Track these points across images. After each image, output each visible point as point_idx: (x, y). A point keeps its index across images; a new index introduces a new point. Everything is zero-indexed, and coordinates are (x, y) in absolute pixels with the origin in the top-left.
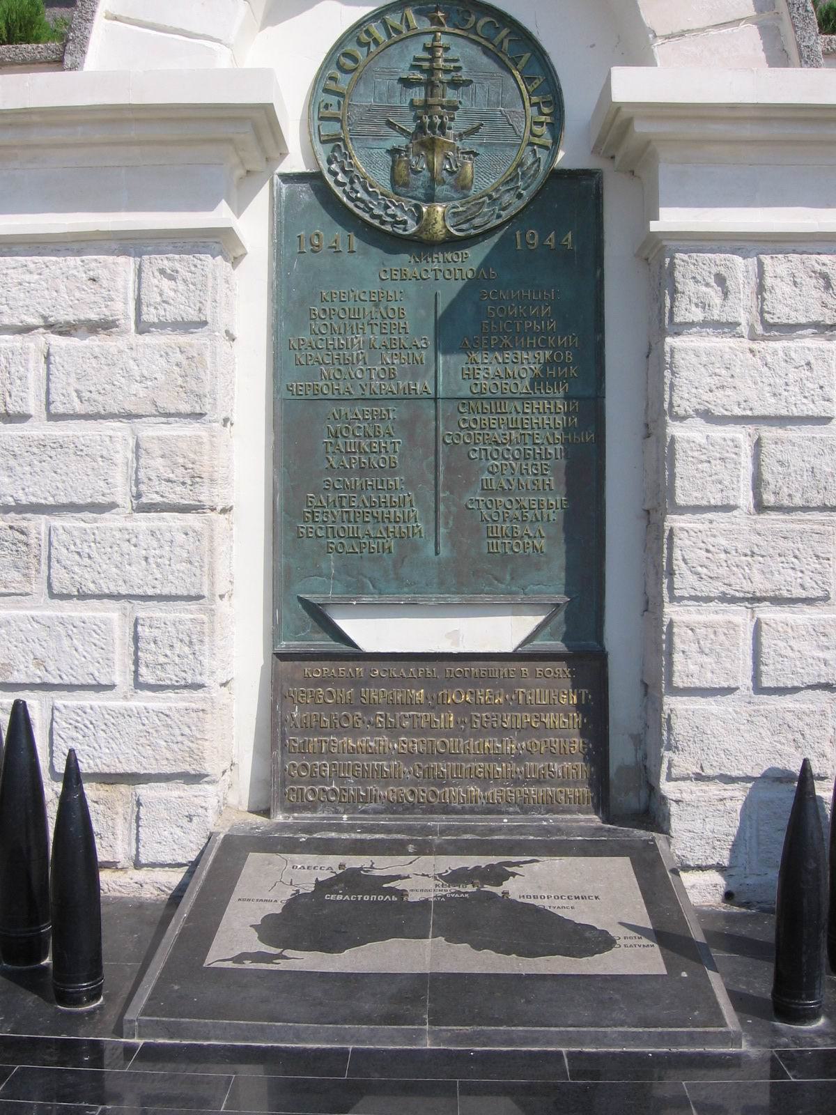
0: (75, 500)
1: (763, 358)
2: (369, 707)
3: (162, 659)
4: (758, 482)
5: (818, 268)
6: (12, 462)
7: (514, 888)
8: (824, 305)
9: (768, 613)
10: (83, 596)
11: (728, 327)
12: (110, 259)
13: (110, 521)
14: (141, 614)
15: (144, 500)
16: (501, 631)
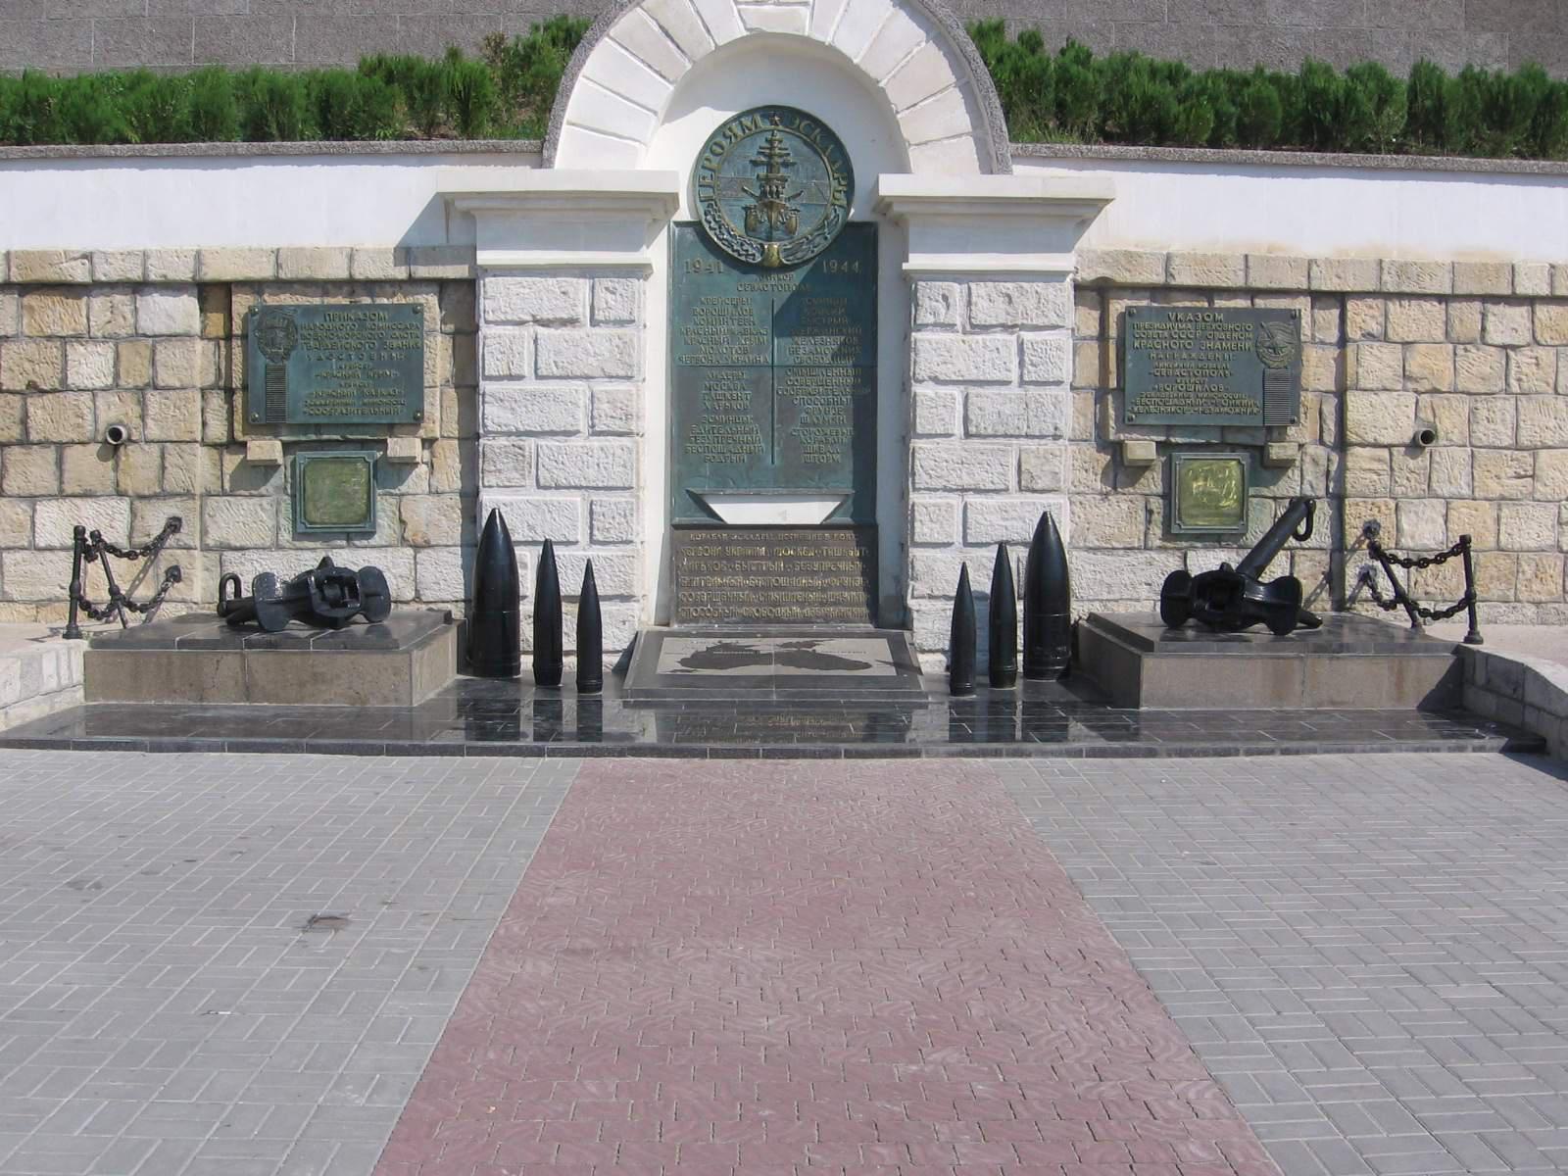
0: (554, 429)
1: (970, 346)
2: (730, 559)
3: (607, 526)
4: (966, 420)
5: (1004, 291)
6: (514, 405)
7: (819, 649)
8: (1008, 314)
9: (971, 498)
10: (558, 487)
11: (949, 327)
12: (575, 280)
13: (575, 442)
14: (594, 499)
15: (597, 429)
16: (813, 511)
